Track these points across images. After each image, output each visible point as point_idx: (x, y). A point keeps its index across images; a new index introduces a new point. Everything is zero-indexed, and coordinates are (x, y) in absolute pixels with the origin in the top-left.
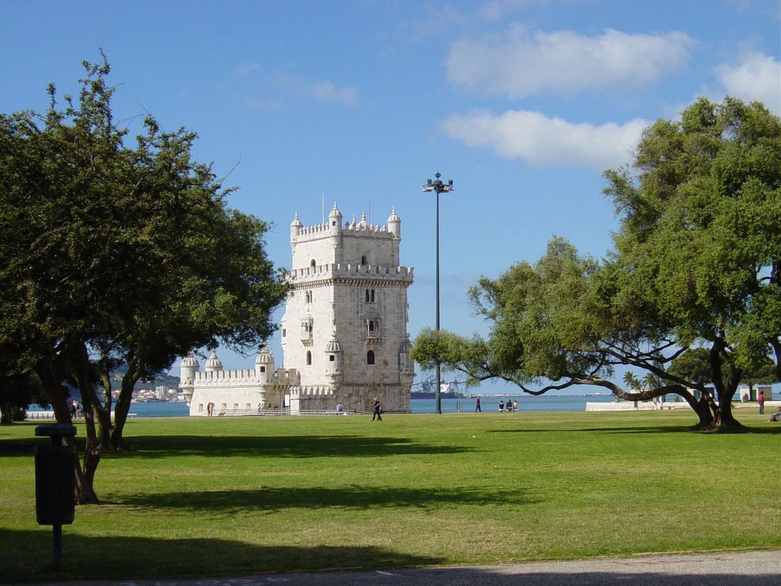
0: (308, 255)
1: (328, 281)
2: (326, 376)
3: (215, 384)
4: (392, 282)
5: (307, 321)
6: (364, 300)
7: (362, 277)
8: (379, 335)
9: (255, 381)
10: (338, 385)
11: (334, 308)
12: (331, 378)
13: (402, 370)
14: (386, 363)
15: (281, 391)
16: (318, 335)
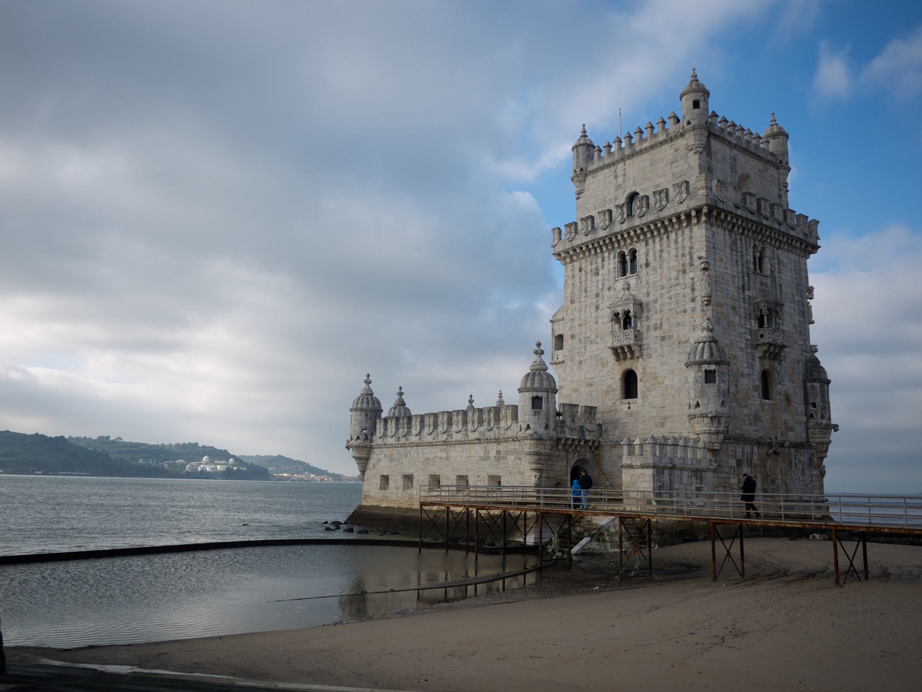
0: (618, 187)
1: (693, 213)
2: (692, 417)
3: (414, 439)
4: (792, 240)
5: (631, 307)
6: (752, 267)
7: (750, 216)
8: (781, 338)
9: (514, 426)
10: (721, 436)
11: (705, 269)
12: (706, 420)
13: (812, 416)
14: (788, 399)
15: (567, 451)
16: (659, 333)
